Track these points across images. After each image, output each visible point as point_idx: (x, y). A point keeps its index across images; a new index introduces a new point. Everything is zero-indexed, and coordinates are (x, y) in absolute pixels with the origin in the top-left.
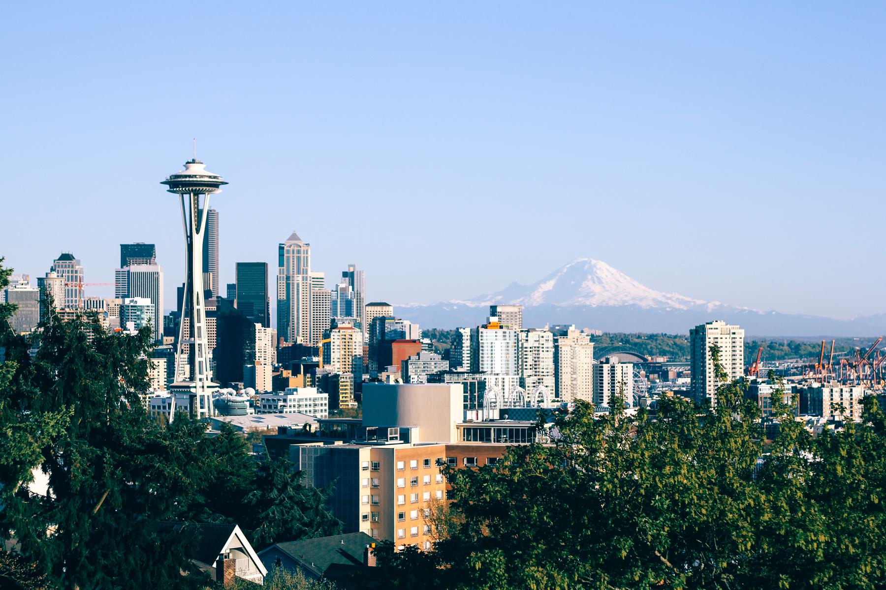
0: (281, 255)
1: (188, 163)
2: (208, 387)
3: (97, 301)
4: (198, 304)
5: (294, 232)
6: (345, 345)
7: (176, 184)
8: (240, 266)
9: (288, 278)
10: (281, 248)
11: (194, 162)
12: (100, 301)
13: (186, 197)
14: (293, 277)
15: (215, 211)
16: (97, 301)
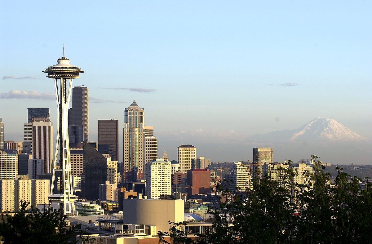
0: (126, 116)
1: (60, 59)
2: (71, 198)
3: (12, 144)
4: (65, 146)
5: (134, 101)
6: (160, 172)
7: (53, 72)
8: (100, 121)
9: (130, 130)
10: (126, 111)
11: (63, 59)
12: (14, 144)
13: (59, 80)
14: (133, 129)
15: (86, 88)
16: (12, 144)
